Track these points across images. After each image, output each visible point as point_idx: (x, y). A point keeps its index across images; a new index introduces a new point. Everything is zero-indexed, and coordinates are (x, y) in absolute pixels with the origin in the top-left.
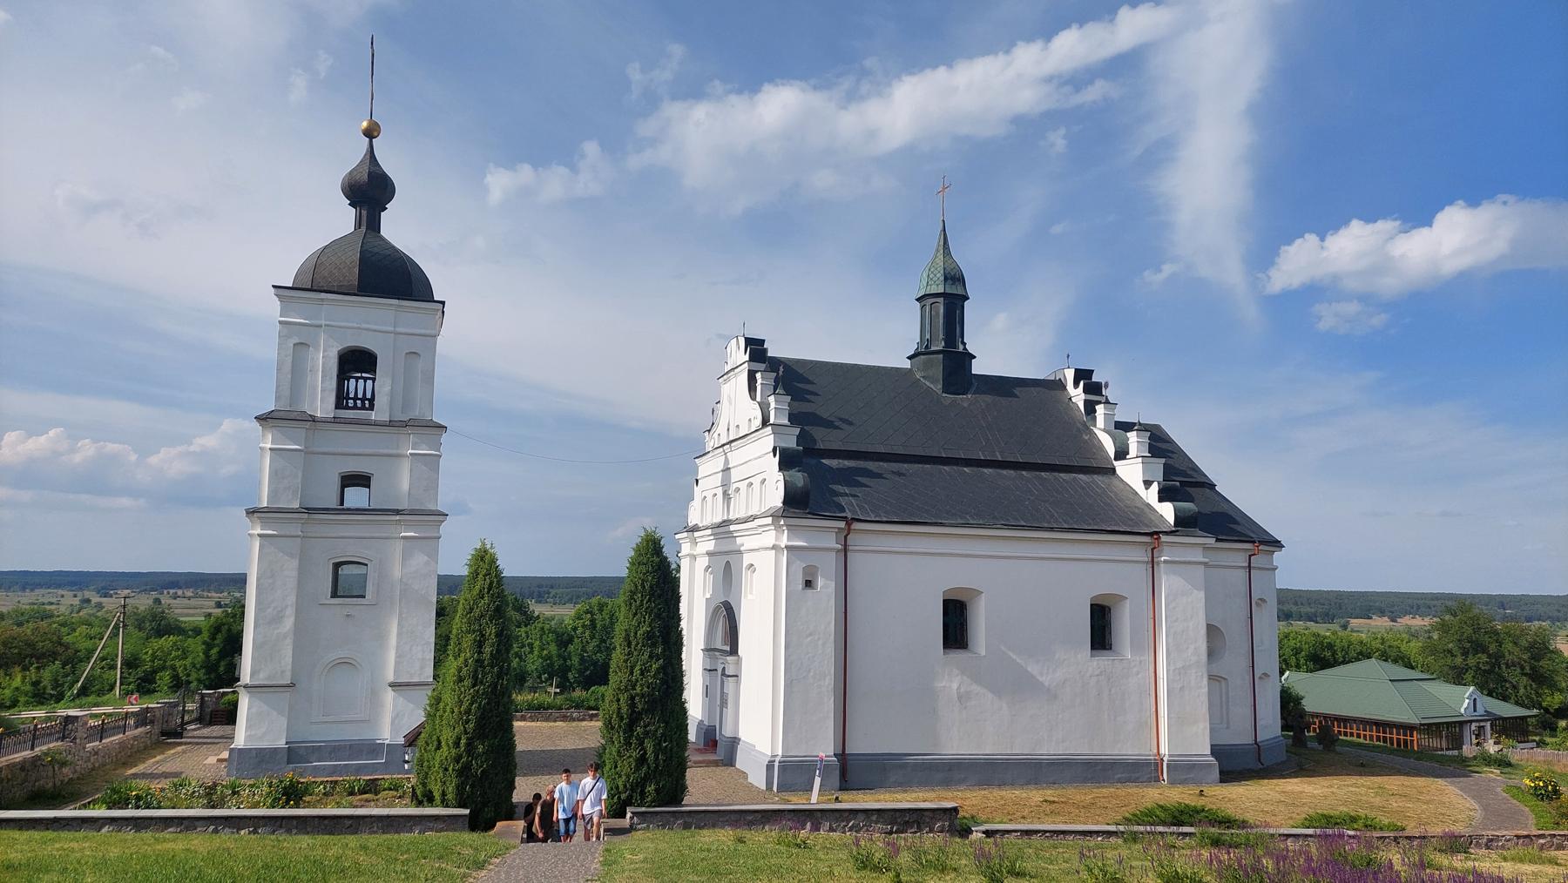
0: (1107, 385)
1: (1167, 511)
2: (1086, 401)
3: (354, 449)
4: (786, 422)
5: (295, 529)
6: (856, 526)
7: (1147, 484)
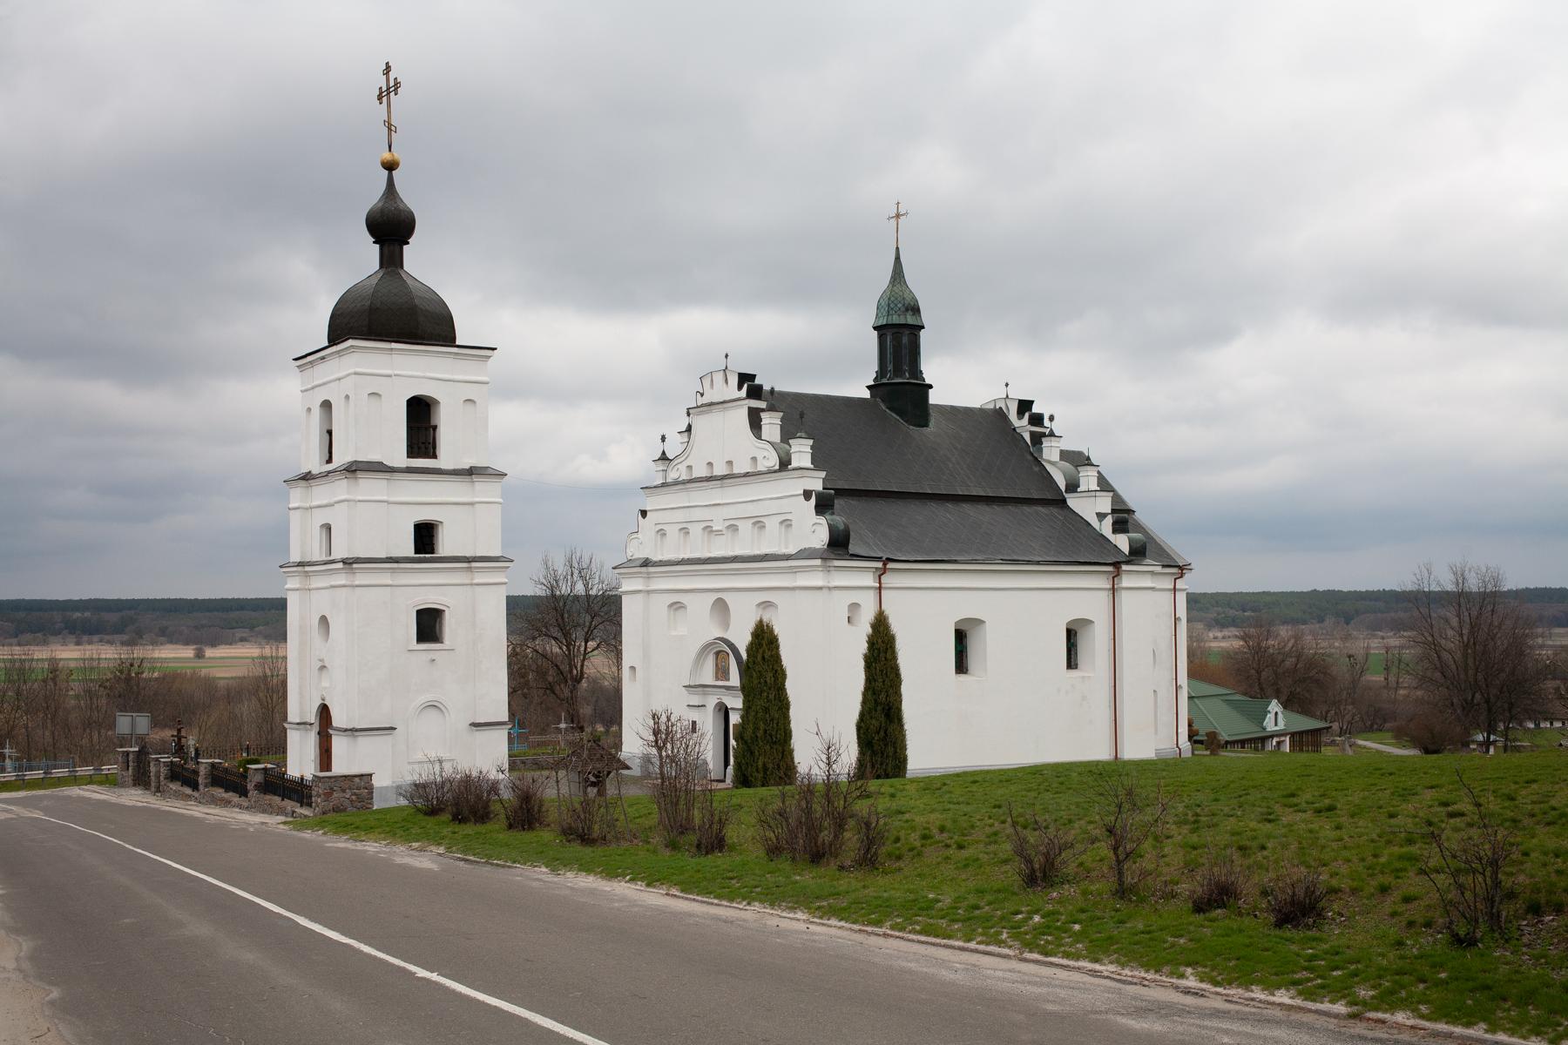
0: (1051, 418)
1: (1122, 542)
2: (1032, 434)
3: (424, 498)
4: (809, 465)
5: (386, 579)
6: (890, 565)
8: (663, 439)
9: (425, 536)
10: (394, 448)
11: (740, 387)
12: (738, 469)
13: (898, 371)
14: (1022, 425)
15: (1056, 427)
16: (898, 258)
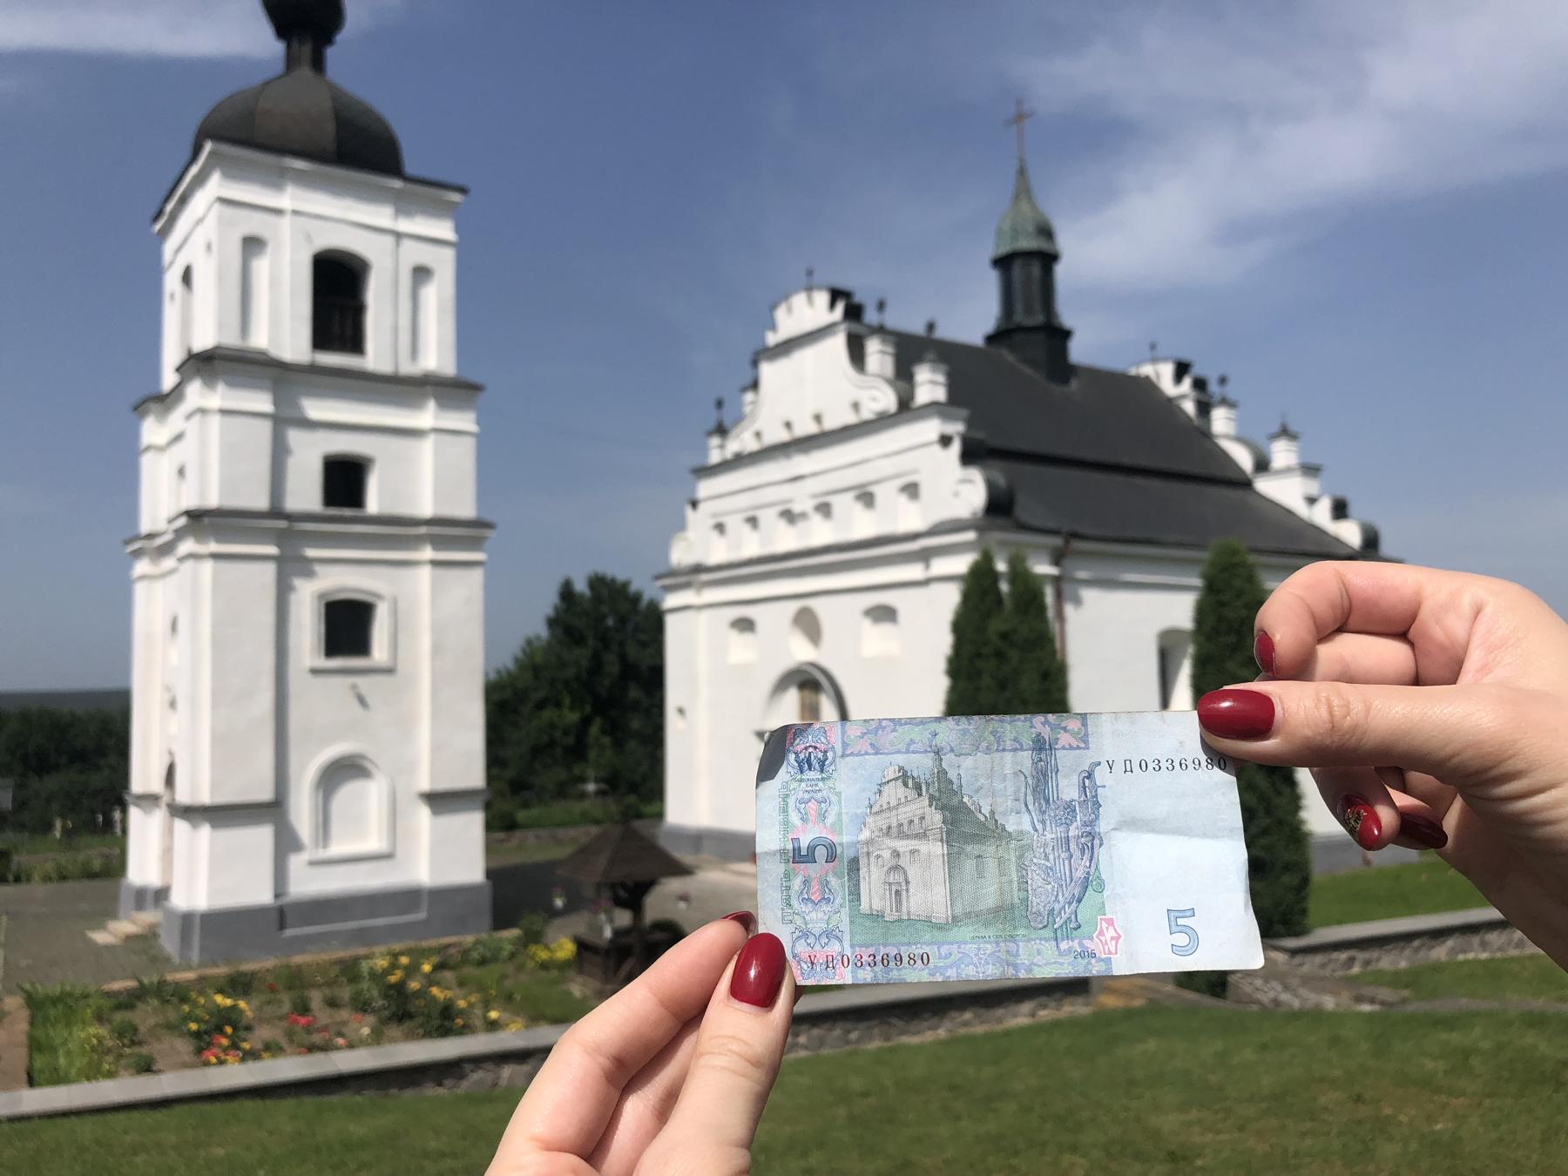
6: (1078, 545)
7: (1311, 501)
8: (719, 404)
9: (345, 479)
10: (283, 328)
11: (832, 305)
12: (830, 423)
13: (1029, 310)
14: (1181, 392)
15: (1231, 391)
16: (1022, 172)
